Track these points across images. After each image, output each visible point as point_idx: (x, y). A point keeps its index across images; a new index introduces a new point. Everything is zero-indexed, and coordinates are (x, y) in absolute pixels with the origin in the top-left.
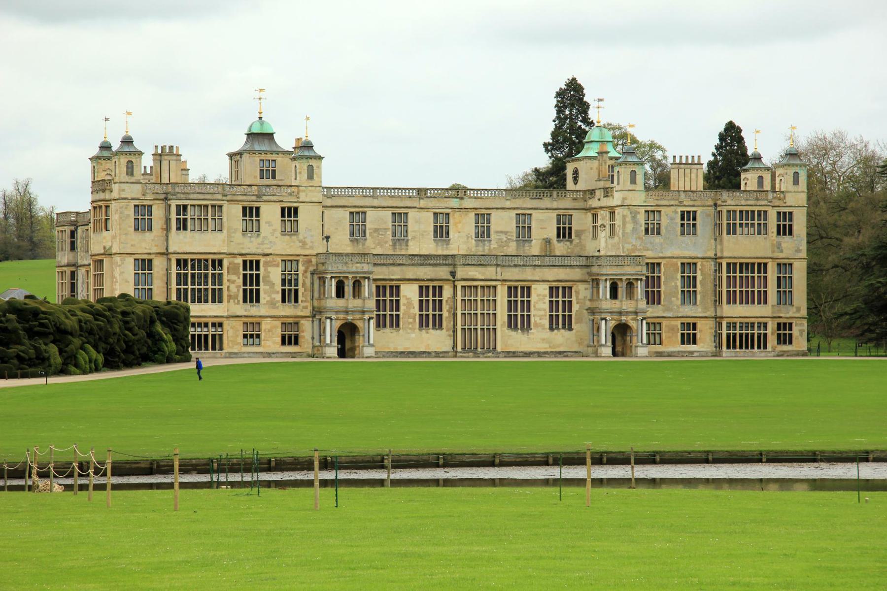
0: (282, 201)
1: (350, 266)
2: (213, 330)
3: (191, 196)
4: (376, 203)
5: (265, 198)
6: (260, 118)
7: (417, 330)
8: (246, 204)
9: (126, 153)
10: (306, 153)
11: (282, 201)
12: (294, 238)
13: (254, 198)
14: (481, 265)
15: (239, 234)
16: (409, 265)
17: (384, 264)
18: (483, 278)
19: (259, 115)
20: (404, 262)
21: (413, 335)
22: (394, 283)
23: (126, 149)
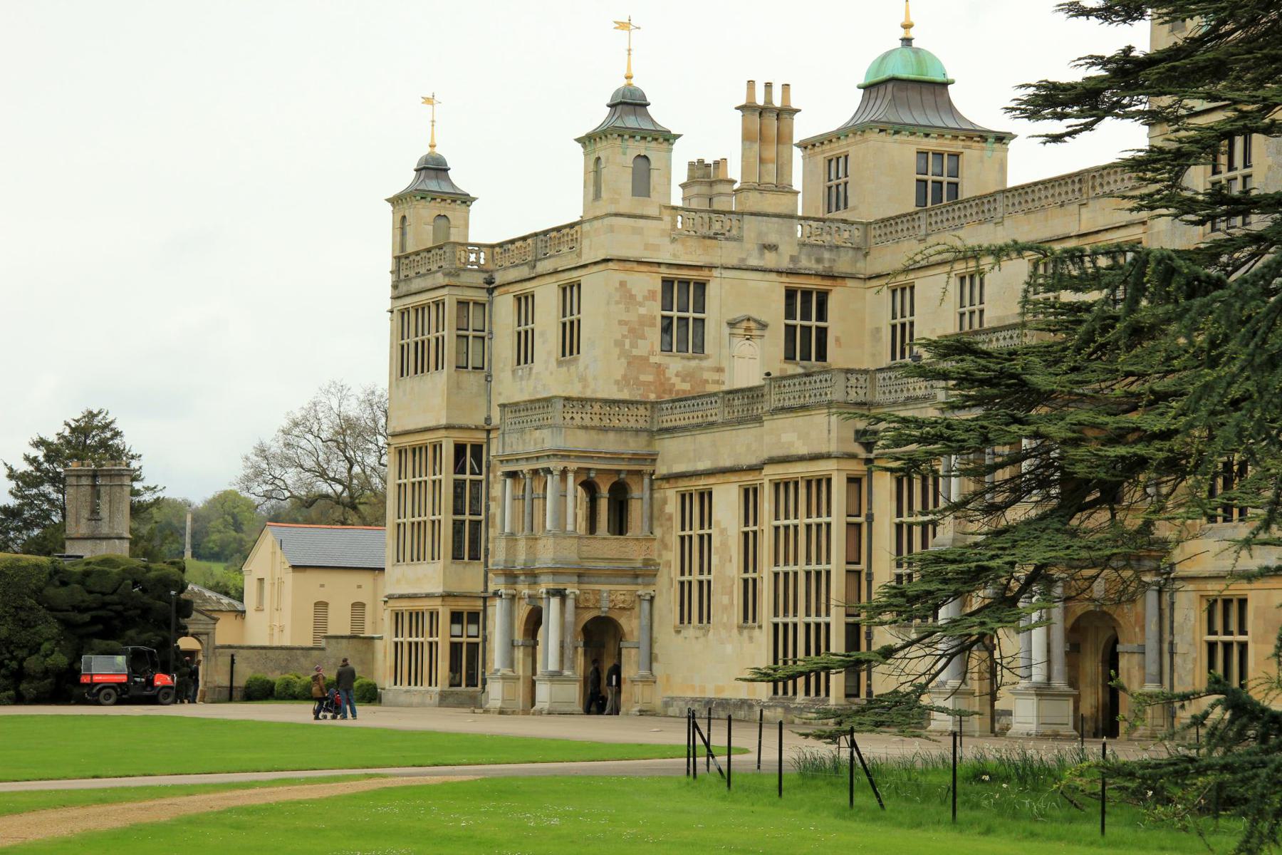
0: (556, 272)
1: (527, 437)
2: (457, 629)
3: (417, 284)
4: (999, 236)
5: (542, 267)
6: (907, 41)
7: (735, 631)
8: (517, 288)
9: (433, 196)
10: (631, 122)
11: (556, 272)
12: (573, 369)
13: (525, 272)
14: (803, 408)
15: (507, 375)
16: (725, 424)
17: (684, 429)
18: (803, 450)
19: (902, 33)
20: (719, 419)
21: (729, 648)
22: (702, 483)
23: (433, 185)
